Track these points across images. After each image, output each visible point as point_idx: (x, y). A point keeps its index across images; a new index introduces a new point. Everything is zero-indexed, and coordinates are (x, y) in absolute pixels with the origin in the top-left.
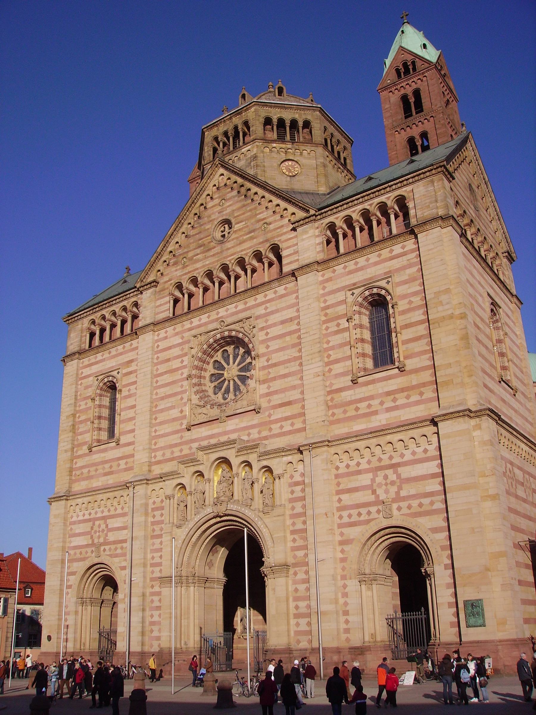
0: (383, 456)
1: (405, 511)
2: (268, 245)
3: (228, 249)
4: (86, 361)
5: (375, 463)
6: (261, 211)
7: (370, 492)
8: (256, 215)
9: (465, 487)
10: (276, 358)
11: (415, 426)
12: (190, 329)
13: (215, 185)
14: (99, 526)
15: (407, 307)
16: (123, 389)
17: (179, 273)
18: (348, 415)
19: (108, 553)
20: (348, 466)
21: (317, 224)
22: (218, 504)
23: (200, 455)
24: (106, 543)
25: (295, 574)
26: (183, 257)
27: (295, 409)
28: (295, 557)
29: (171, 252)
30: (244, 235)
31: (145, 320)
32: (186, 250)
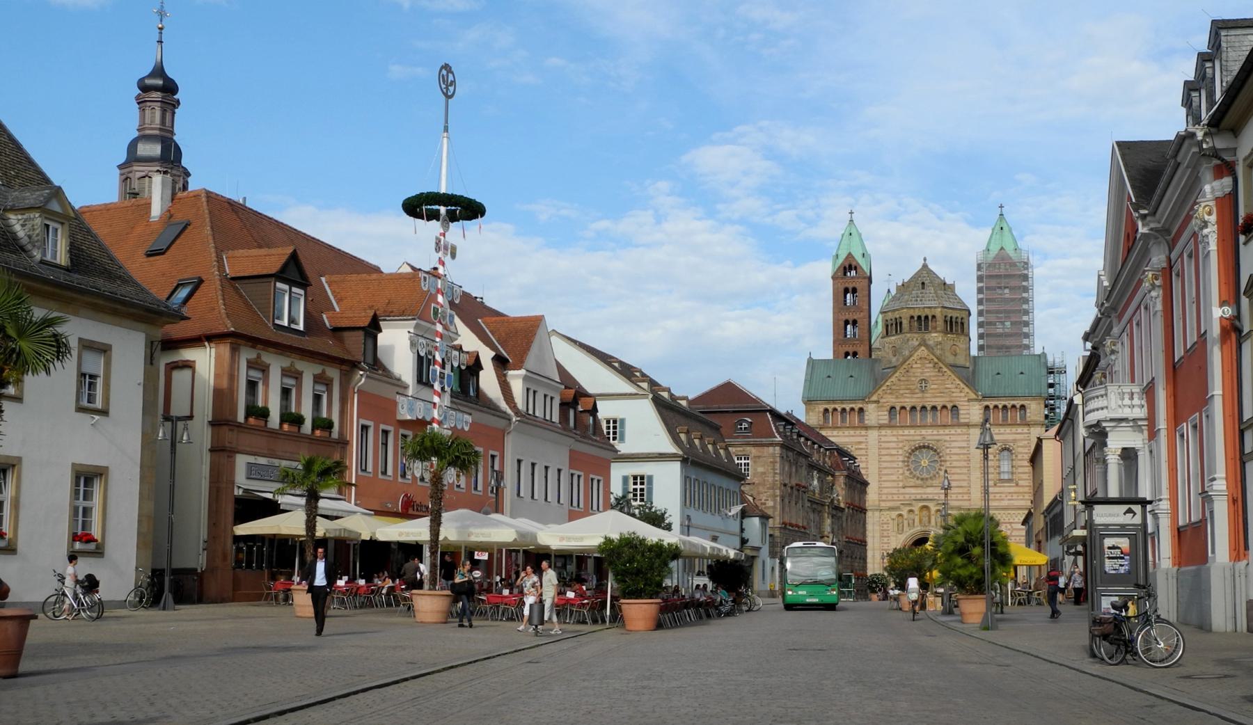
2: (952, 404)
3: (927, 397)
10: (955, 464)
12: (903, 435)
17: (894, 400)
21: (981, 403)
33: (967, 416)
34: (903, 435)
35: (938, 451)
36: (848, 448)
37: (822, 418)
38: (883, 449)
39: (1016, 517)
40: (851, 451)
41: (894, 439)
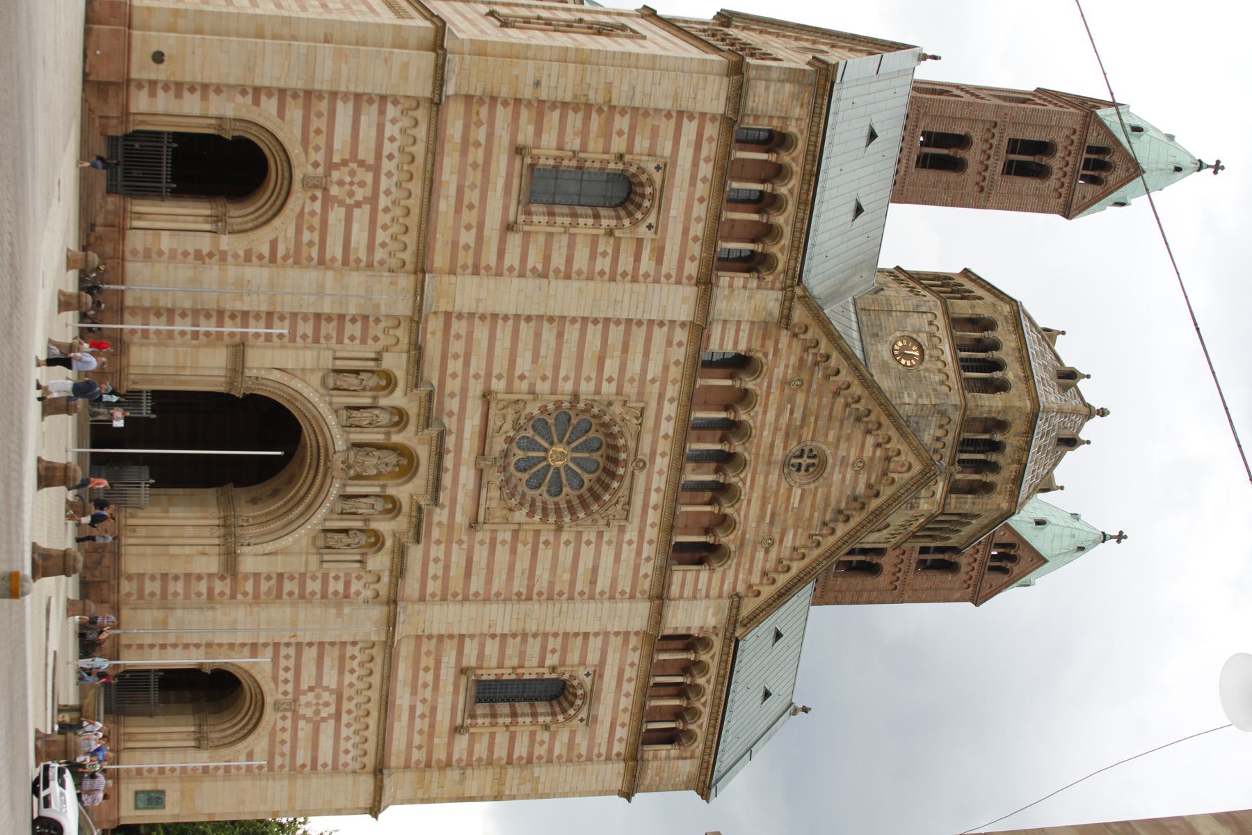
0: (354, 702)
1: (280, 724)
2: (732, 548)
3: (767, 476)
4: (711, 130)
5: (347, 692)
6: (798, 536)
7: (313, 684)
8: (796, 528)
9: (291, 799)
10: (545, 555)
11: (380, 747)
12: (661, 397)
13: (899, 453)
14: (362, 184)
15: (538, 738)
16: (612, 240)
17: (779, 372)
18: (423, 657)
19: (307, 210)
20: (353, 657)
22: (344, 466)
23: (433, 431)
24: (327, 201)
25: (222, 578)
26: (805, 382)
27: (456, 584)
28: (246, 577)
29: (828, 357)
30: (775, 506)
31: (724, 298)
32: (814, 386)
33: (688, 592)
34: (661, 397)
35: (595, 507)
36: (647, 213)
37: (764, 124)
38: (627, 333)
39: (356, 732)
40: (635, 223)
41: (654, 370)
